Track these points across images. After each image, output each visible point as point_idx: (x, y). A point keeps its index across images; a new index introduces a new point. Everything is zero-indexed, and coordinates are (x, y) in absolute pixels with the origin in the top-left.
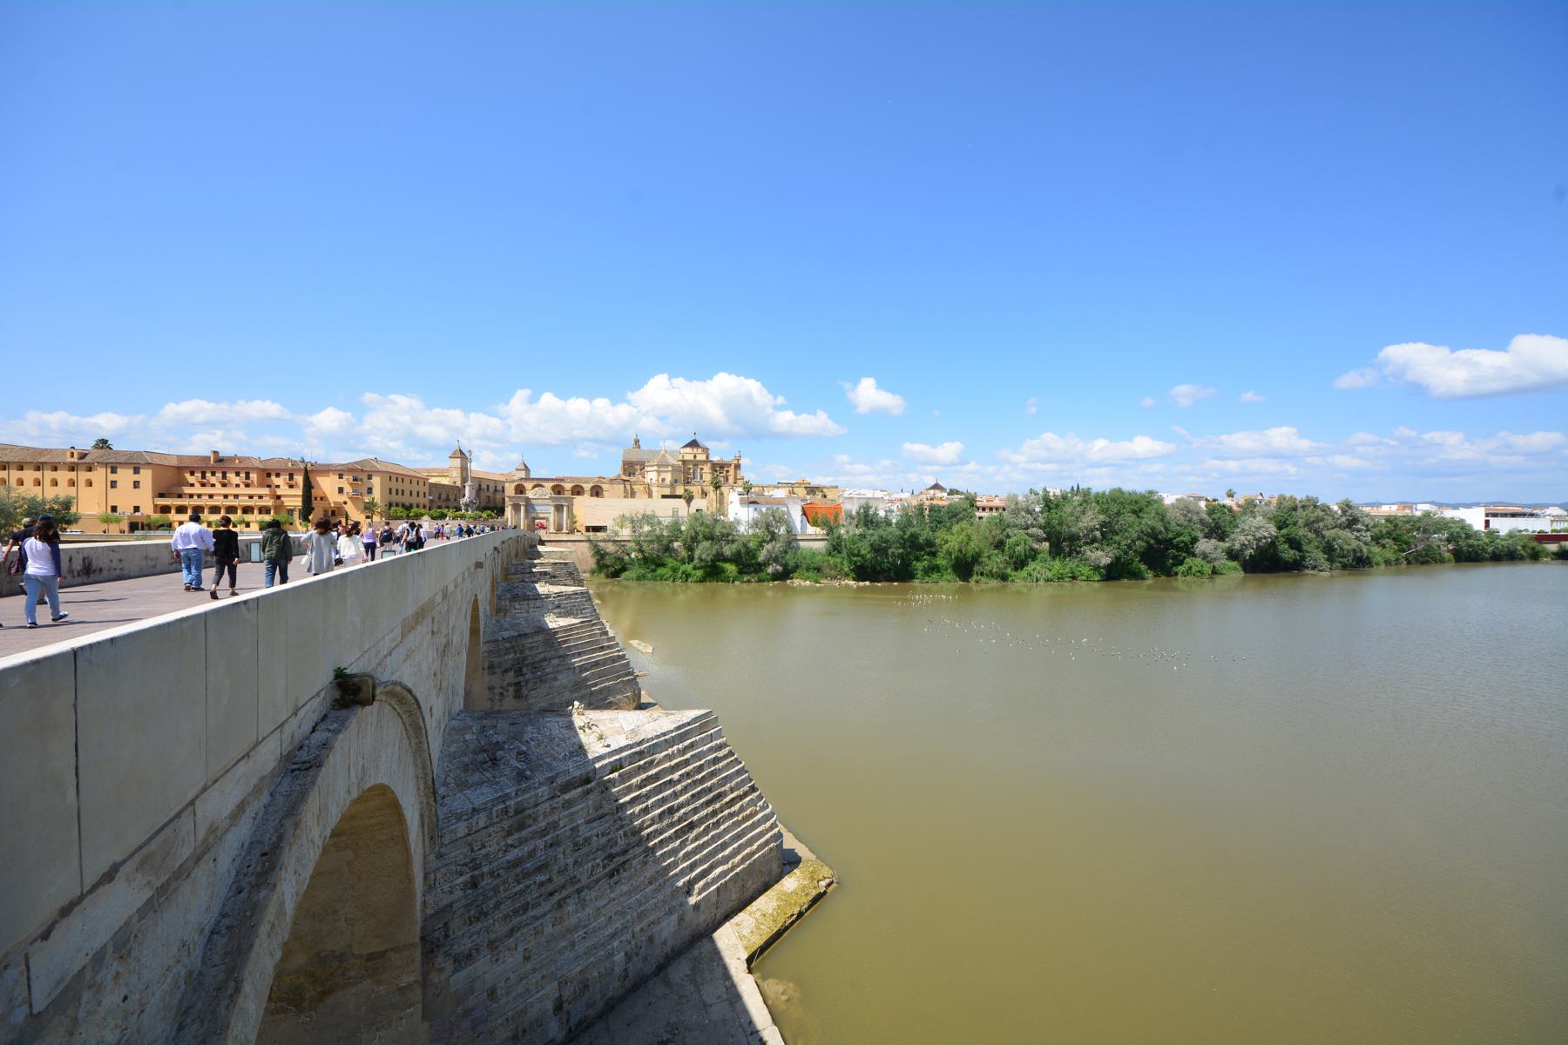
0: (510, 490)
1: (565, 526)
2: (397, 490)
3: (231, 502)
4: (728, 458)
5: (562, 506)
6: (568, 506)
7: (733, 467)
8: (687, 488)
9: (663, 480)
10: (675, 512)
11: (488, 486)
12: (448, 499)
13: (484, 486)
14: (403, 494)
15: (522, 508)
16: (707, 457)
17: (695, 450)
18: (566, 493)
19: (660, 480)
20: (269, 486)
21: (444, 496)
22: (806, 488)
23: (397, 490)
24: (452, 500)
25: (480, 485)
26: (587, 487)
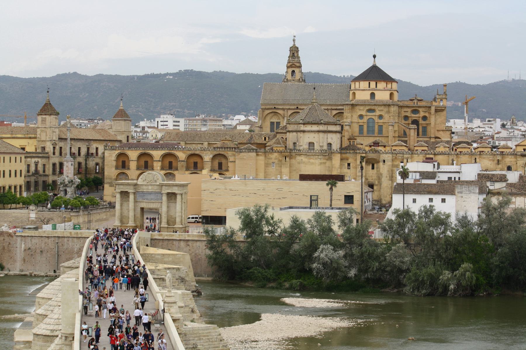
0: (111, 157)
5: (174, 195)
7: (433, 109)
8: (344, 156)
10: (313, 201)
11: (79, 148)
15: (132, 197)
17: (373, 84)
18: (180, 165)
19: (307, 147)
21: (33, 169)
24: (41, 172)
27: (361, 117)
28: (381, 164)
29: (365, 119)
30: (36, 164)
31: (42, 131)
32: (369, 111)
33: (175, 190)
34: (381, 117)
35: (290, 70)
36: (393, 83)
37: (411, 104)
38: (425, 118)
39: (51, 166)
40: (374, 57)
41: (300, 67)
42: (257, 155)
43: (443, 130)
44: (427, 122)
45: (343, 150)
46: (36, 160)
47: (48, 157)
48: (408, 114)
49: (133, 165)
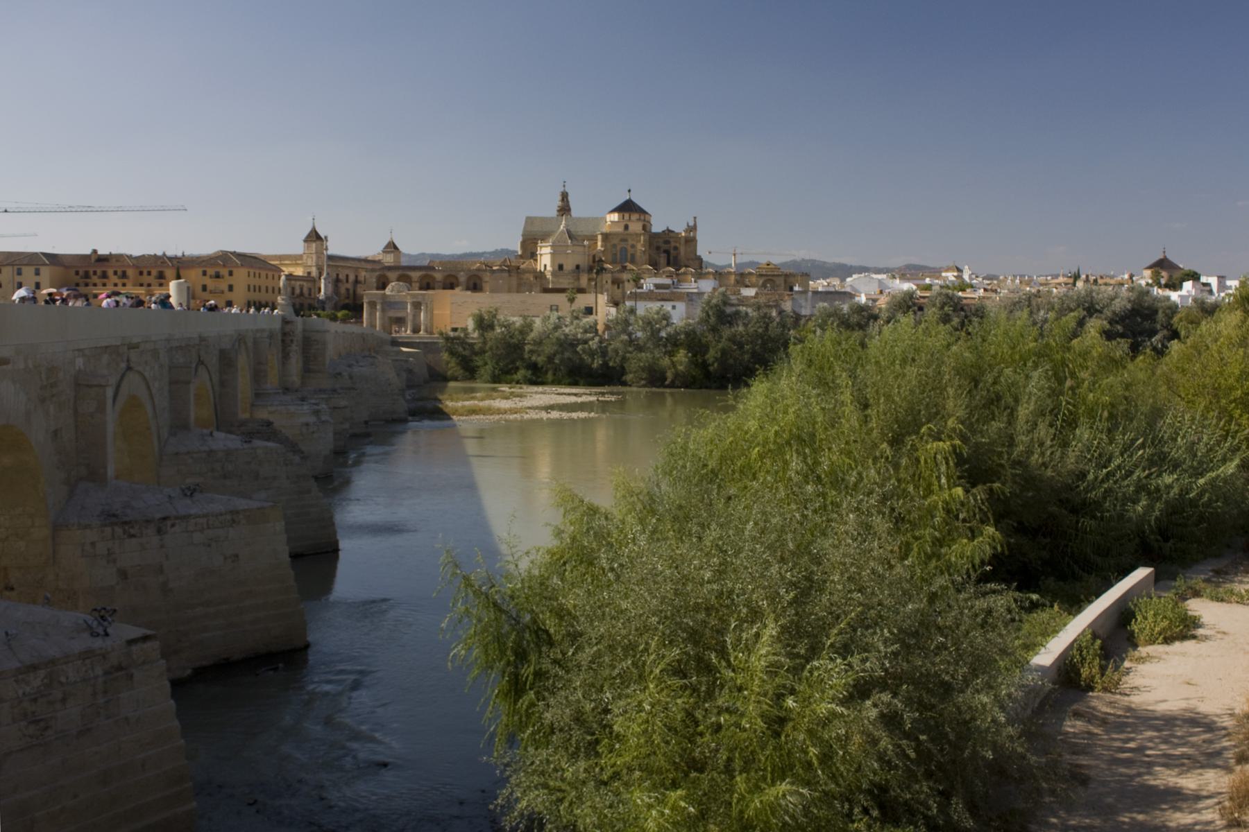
1: (422, 328)
2: (255, 286)
4: (679, 228)
9: (561, 267)
11: (347, 276)
12: (302, 294)
13: (342, 277)
14: (260, 291)
15: (378, 307)
17: (627, 216)
19: (557, 268)
20: (141, 285)
22: (761, 275)
23: (255, 286)
25: (338, 275)
26: (462, 277)
27: (614, 246)
29: (618, 248)
31: (308, 257)
36: (647, 216)
39: (317, 290)
40: (629, 191)
42: (510, 276)
43: (692, 259)
46: (301, 283)
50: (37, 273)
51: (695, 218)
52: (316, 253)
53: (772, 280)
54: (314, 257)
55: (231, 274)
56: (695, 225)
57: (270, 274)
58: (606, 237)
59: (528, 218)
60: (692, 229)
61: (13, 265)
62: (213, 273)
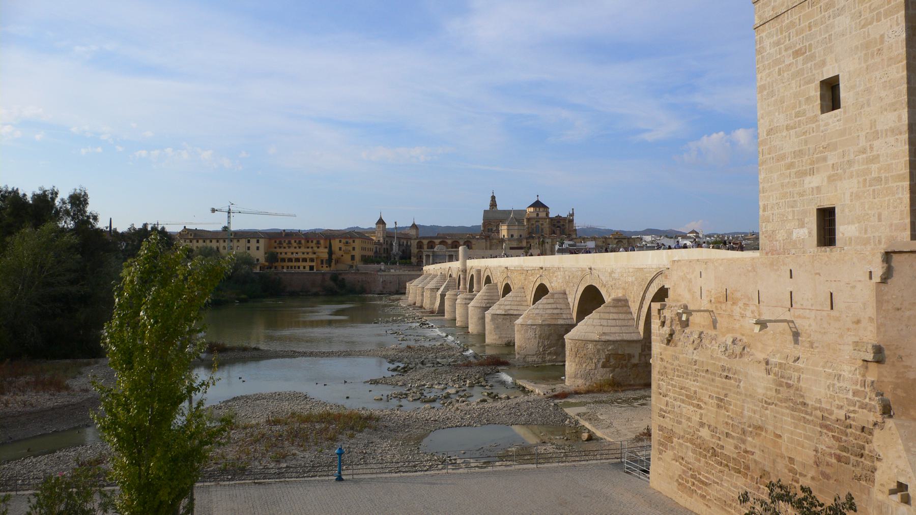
3: (295, 256)
4: (564, 215)
5: (453, 255)
6: (455, 256)
8: (528, 241)
9: (512, 236)
16: (547, 214)
17: (538, 209)
20: (308, 248)
22: (615, 239)
27: (533, 224)
28: (546, 244)
29: (534, 226)
30: (376, 248)
32: (537, 221)
33: (453, 253)
34: (542, 224)
35: (492, 207)
37: (557, 218)
38: (563, 225)
40: (538, 196)
41: (496, 206)
42: (486, 241)
44: (564, 227)
45: (527, 239)
46: (376, 246)
47: (382, 245)
48: (556, 223)
49: (425, 247)
50: (258, 242)
51: (573, 209)
52: (383, 230)
53: (621, 241)
54: (382, 232)
55: (354, 242)
56: (573, 213)
57: (369, 241)
58: (529, 220)
59: (484, 211)
60: (572, 215)
61: (246, 238)
62: (345, 242)
